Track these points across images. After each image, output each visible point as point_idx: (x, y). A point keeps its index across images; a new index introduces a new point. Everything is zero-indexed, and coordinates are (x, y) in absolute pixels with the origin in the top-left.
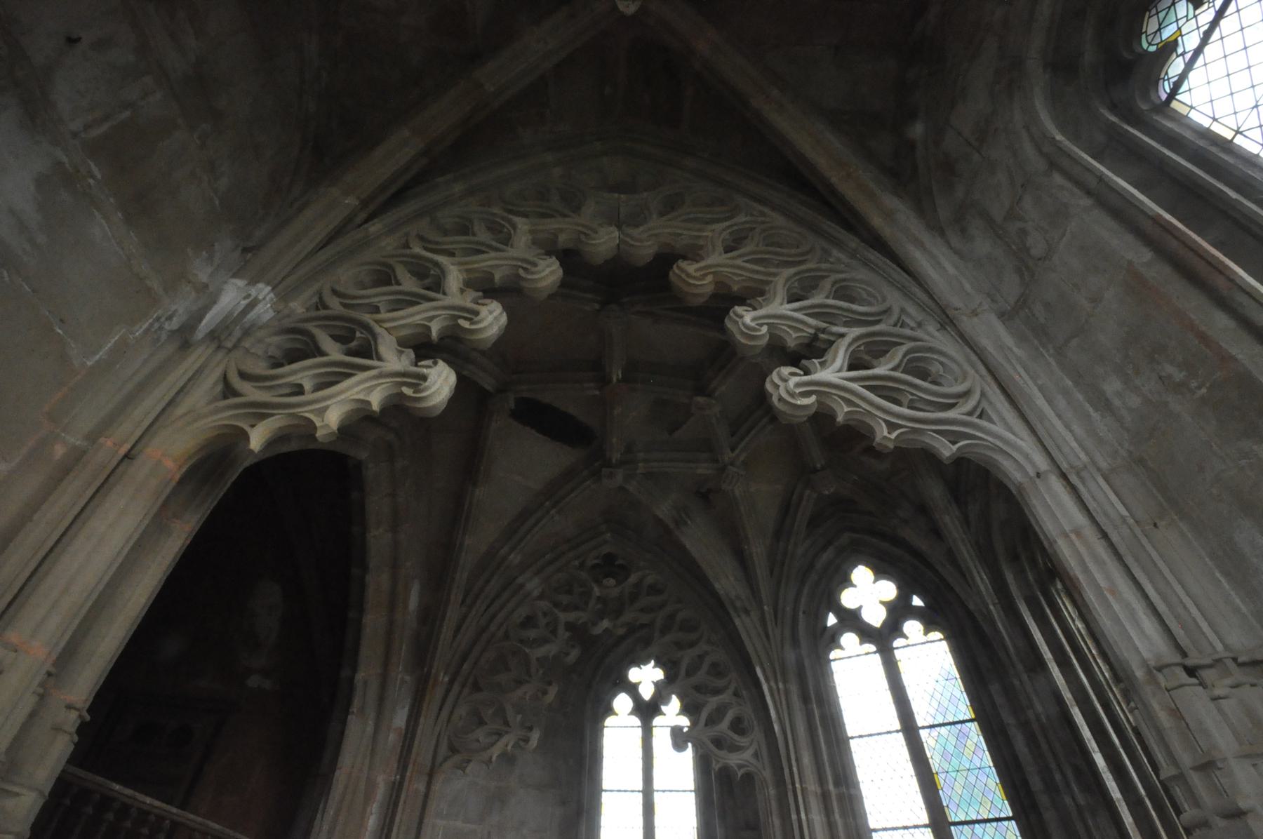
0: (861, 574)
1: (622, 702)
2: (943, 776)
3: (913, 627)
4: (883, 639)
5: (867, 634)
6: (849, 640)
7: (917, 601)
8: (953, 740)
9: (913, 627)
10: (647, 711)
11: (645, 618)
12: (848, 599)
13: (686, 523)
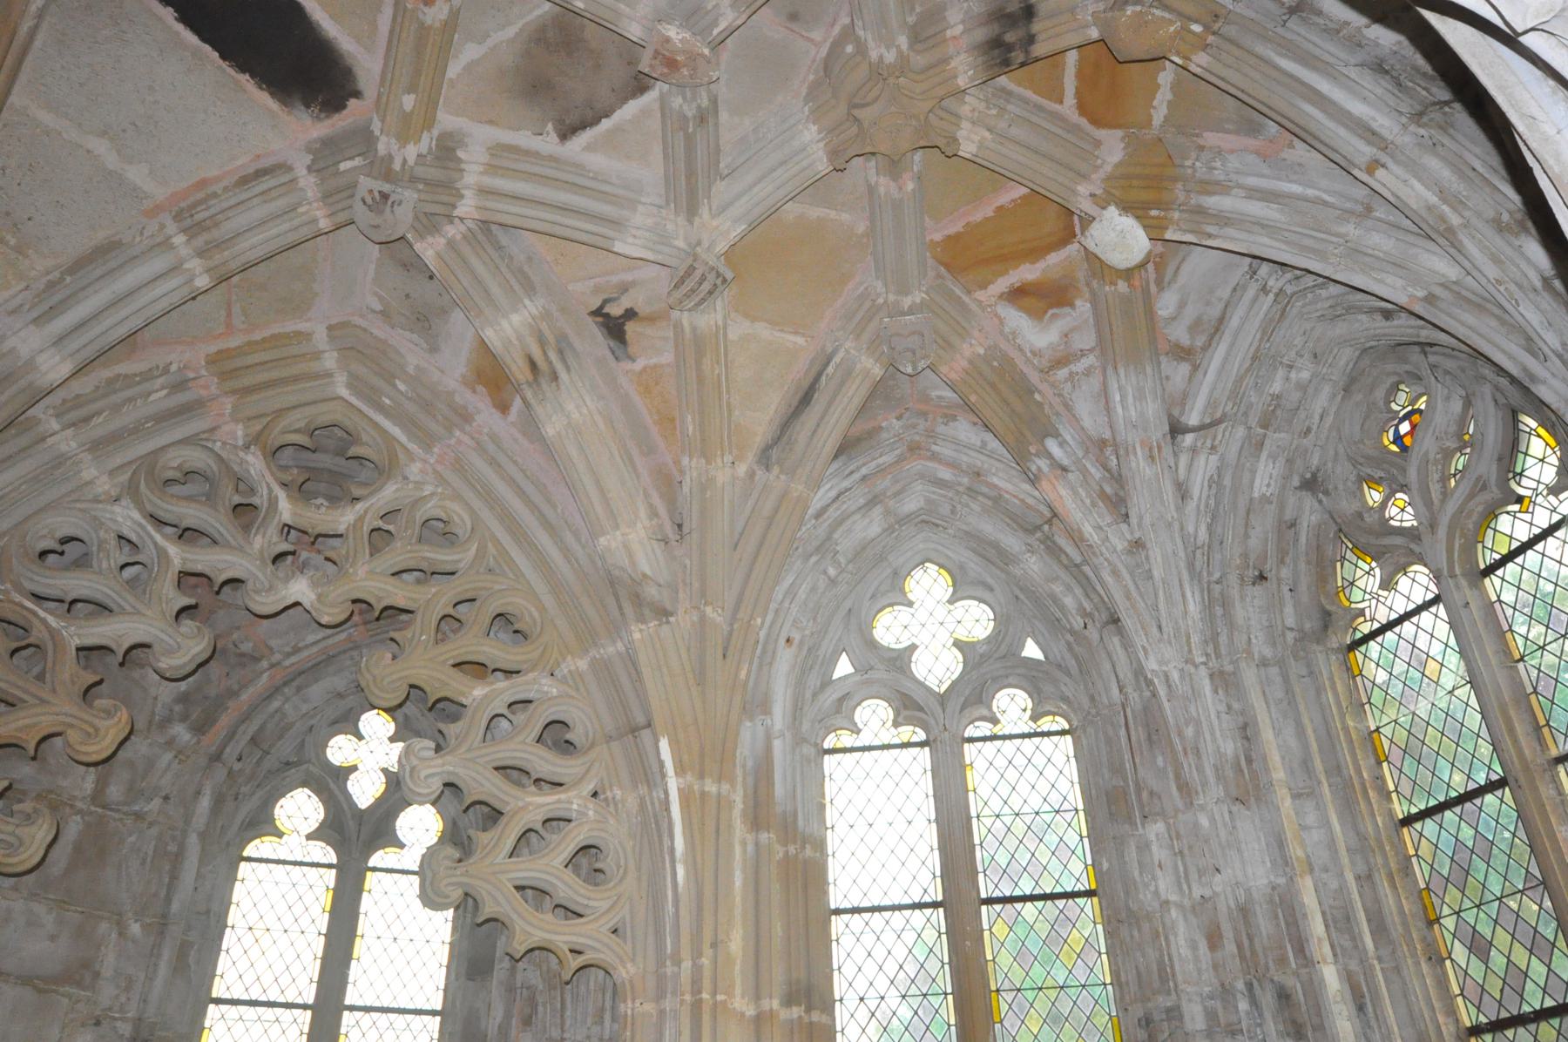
0: (928, 584)
1: (300, 810)
2: (1009, 997)
3: (1012, 705)
4: (942, 722)
5: (910, 704)
6: (874, 717)
7: (1032, 650)
8: (1043, 928)
9: (1012, 705)
10: (356, 835)
11: (399, 593)
12: (889, 629)
13: (555, 377)
